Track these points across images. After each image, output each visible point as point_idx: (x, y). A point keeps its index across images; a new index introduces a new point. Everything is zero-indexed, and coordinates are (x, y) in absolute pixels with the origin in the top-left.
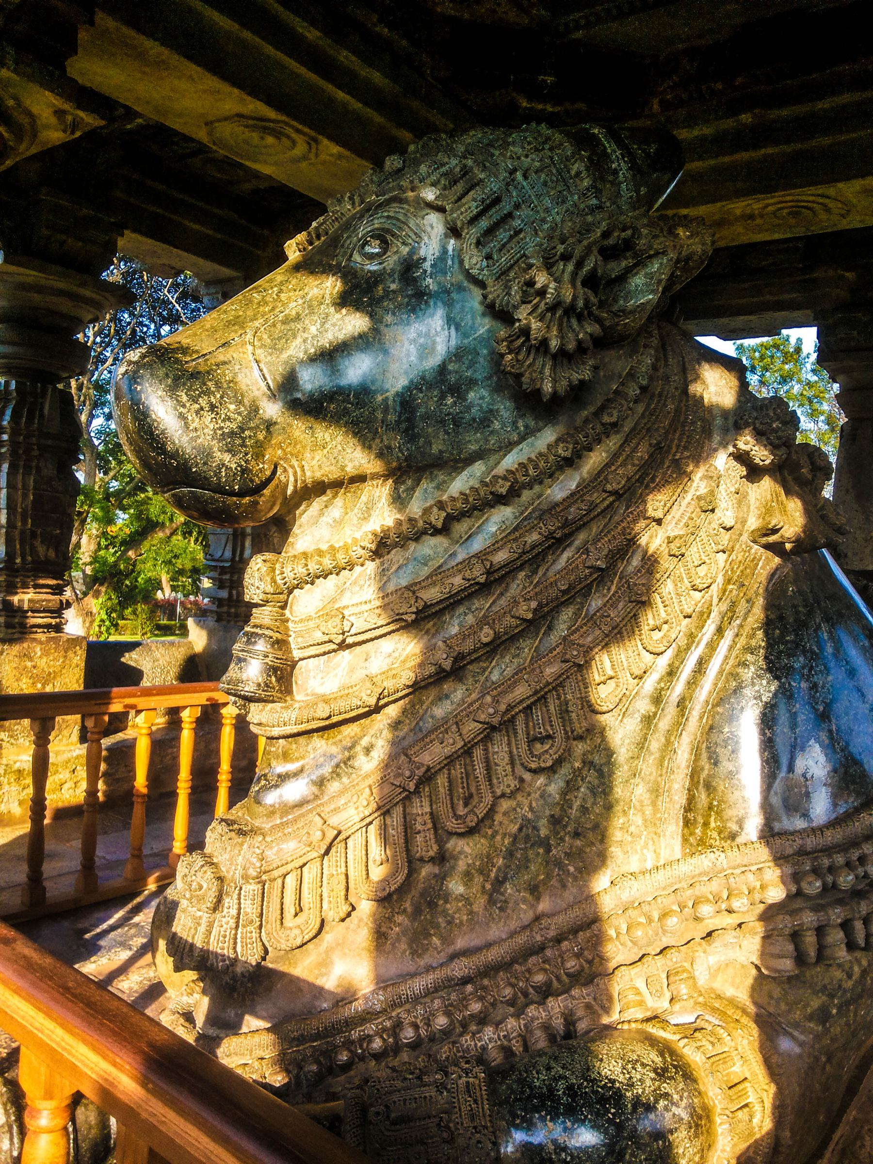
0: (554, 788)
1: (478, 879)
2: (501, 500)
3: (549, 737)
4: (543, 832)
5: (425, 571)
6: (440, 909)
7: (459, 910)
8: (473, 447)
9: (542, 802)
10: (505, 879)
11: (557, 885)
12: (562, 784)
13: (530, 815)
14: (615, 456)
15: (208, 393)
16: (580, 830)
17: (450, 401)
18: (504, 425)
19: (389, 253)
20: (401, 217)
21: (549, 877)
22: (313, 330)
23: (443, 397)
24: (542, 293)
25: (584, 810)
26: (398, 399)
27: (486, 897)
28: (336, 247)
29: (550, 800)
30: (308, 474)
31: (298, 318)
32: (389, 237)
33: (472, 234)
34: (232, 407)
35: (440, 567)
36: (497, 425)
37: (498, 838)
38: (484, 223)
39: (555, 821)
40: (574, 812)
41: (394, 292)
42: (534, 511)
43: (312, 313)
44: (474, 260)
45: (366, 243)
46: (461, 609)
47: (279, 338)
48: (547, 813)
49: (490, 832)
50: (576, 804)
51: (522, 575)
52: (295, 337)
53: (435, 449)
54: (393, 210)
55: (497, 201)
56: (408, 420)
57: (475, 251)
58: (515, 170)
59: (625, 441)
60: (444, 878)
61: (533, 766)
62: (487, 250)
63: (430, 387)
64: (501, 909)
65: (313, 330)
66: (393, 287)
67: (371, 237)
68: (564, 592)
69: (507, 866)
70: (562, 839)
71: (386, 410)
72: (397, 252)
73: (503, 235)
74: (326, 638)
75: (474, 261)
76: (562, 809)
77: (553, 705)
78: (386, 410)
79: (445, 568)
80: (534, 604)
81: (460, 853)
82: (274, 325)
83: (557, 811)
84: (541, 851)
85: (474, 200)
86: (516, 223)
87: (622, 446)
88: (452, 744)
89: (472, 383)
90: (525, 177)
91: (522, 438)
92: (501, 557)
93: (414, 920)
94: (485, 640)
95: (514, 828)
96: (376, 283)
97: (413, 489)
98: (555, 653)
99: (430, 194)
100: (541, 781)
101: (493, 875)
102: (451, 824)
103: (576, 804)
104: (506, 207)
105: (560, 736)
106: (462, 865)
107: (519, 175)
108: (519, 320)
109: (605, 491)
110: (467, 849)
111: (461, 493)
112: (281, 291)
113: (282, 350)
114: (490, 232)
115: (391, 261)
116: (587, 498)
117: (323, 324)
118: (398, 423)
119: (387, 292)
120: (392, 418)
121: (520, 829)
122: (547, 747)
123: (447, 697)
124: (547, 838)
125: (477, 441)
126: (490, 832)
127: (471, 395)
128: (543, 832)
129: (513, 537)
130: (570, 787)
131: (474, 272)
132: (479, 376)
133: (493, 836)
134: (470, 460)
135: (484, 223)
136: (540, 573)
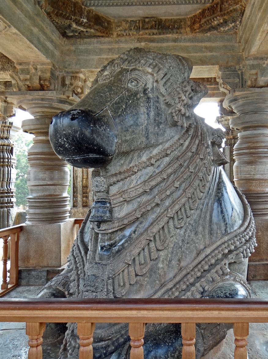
0: (182, 232)
1: (165, 262)
2: (167, 155)
3: (182, 218)
4: (180, 244)
5: (147, 177)
6: (157, 273)
7: (162, 271)
8: (161, 141)
9: (179, 236)
10: (172, 260)
11: (185, 258)
12: (184, 230)
13: (176, 241)
14: (190, 143)
15: (103, 126)
16: (188, 242)
17: (156, 128)
18: (167, 135)
19: (139, 86)
20: (140, 75)
21: (182, 256)
22: (124, 106)
23: (155, 127)
24: (183, 101)
25: (189, 236)
26: (145, 128)
27: (167, 266)
28: (121, 81)
29: (181, 235)
30: (122, 150)
31: (119, 103)
32: (138, 81)
33: (162, 83)
34: (108, 130)
35: (151, 175)
36: (166, 135)
37: (169, 249)
38: (164, 80)
39: (183, 241)
40: (186, 237)
41: (142, 97)
42: (174, 158)
43: (122, 102)
44: (163, 90)
45: (132, 82)
46: (158, 187)
47: (116, 109)
48: (181, 239)
49: (167, 248)
50: (187, 235)
51: (172, 175)
52: (120, 109)
53: (152, 142)
54: (137, 72)
55: (166, 74)
56: (147, 134)
57: (163, 88)
58: (171, 66)
59: (191, 139)
60: (157, 264)
61: (179, 227)
62: (166, 88)
63: (152, 125)
64: (172, 268)
65: (124, 106)
66: (142, 95)
67: (134, 80)
68: (185, 179)
69: (171, 256)
70: (184, 245)
71: (142, 131)
72: (141, 85)
73: (169, 84)
75: (163, 90)
76: (184, 237)
77: (183, 210)
78: (142, 131)
79: (153, 175)
80: (179, 183)
81: (161, 256)
82: (113, 104)
83: (183, 238)
84: (180, 250)
85: (162, 73)
86: (171, 81)
87: (191, 140)
88: (162, 224)
89: (161, 123)
90: (173, 69)
91: (171, 138)
92: (170, 171)
93: (150, 278)
94: (168, 194)
95: (172, 245)
96: (137, 94)
97: (143, 153)
98: (183, 195)
99: (150, 70)
100: (178, 231)
101: (168, 260)
102: (160, 248)
103: (187, 235)
104: (168, 76)
105: (185, 217)
106: (161, 259)
107: (171, 68)
108: (177, 107)
109: (191, 152)
110: (162, 254)
111: (156, 154)
112: (110, 94)
113: (118, 113)
114: (165, 83)
115: (140, 89)
116: (187, 154)
117: (126, 105)
118: (145, 134)
119: (141, 97)
120: (144, 133)
121: (174, 245)
122: (181, 221)
123: (155, 212)
124: (181, 246)
125: (162, 139)
126: (167, 248)
127: (161, 127)
128: (180, 244)
129: (170, 165)
130: (186, 231)
131: (163, 93)
132: (162, 122)
133: (168, 249)
134: (158, 145)
135: (164, 80)
136: (176, 175)
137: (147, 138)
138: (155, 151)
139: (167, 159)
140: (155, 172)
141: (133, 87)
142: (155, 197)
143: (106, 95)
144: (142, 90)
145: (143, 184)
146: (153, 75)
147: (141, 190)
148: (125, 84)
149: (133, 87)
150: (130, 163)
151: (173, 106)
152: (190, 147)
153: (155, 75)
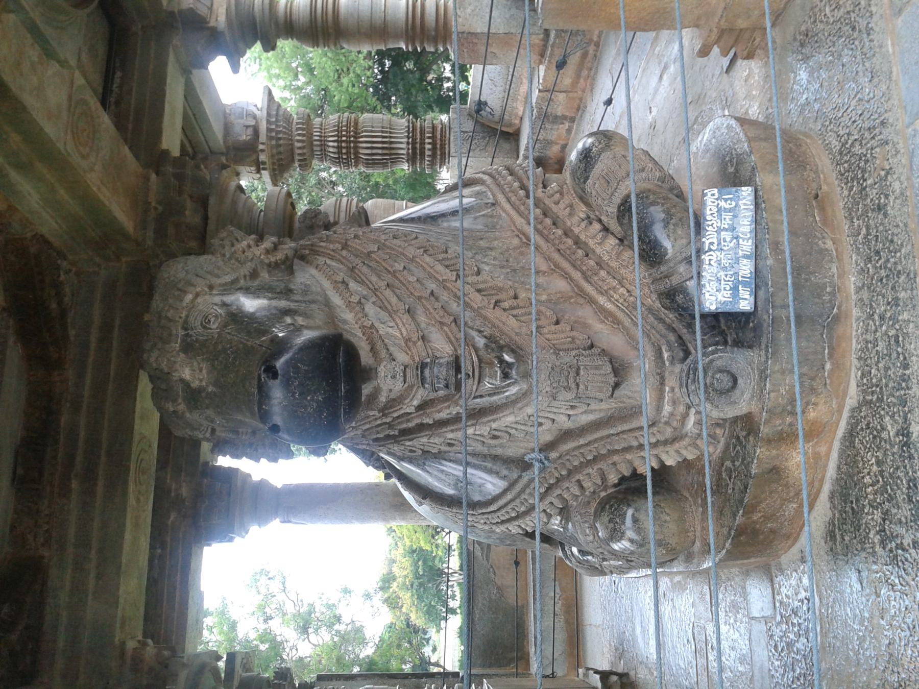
8: (319, 289)
35: (380, 308)
36: (308, 282)
65: (255, 325)
74: (421, 340)
132: (284, 285)
137: (313, 302)
138: (337, 300)
139: (353, 285)
140: (374, 303)
141: (220, 320)
142: (420, 298)
143: (232, 353)
144: (225, 308)
145: (395, 317)
146: (197, 295)
147: (406, 317)
148: (213, 333)
149: (220, 320)
150: (356, 335)
151: (256, 265)
152: (332, 253)
153: (199, 289)
